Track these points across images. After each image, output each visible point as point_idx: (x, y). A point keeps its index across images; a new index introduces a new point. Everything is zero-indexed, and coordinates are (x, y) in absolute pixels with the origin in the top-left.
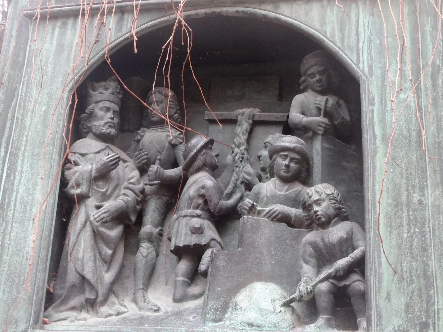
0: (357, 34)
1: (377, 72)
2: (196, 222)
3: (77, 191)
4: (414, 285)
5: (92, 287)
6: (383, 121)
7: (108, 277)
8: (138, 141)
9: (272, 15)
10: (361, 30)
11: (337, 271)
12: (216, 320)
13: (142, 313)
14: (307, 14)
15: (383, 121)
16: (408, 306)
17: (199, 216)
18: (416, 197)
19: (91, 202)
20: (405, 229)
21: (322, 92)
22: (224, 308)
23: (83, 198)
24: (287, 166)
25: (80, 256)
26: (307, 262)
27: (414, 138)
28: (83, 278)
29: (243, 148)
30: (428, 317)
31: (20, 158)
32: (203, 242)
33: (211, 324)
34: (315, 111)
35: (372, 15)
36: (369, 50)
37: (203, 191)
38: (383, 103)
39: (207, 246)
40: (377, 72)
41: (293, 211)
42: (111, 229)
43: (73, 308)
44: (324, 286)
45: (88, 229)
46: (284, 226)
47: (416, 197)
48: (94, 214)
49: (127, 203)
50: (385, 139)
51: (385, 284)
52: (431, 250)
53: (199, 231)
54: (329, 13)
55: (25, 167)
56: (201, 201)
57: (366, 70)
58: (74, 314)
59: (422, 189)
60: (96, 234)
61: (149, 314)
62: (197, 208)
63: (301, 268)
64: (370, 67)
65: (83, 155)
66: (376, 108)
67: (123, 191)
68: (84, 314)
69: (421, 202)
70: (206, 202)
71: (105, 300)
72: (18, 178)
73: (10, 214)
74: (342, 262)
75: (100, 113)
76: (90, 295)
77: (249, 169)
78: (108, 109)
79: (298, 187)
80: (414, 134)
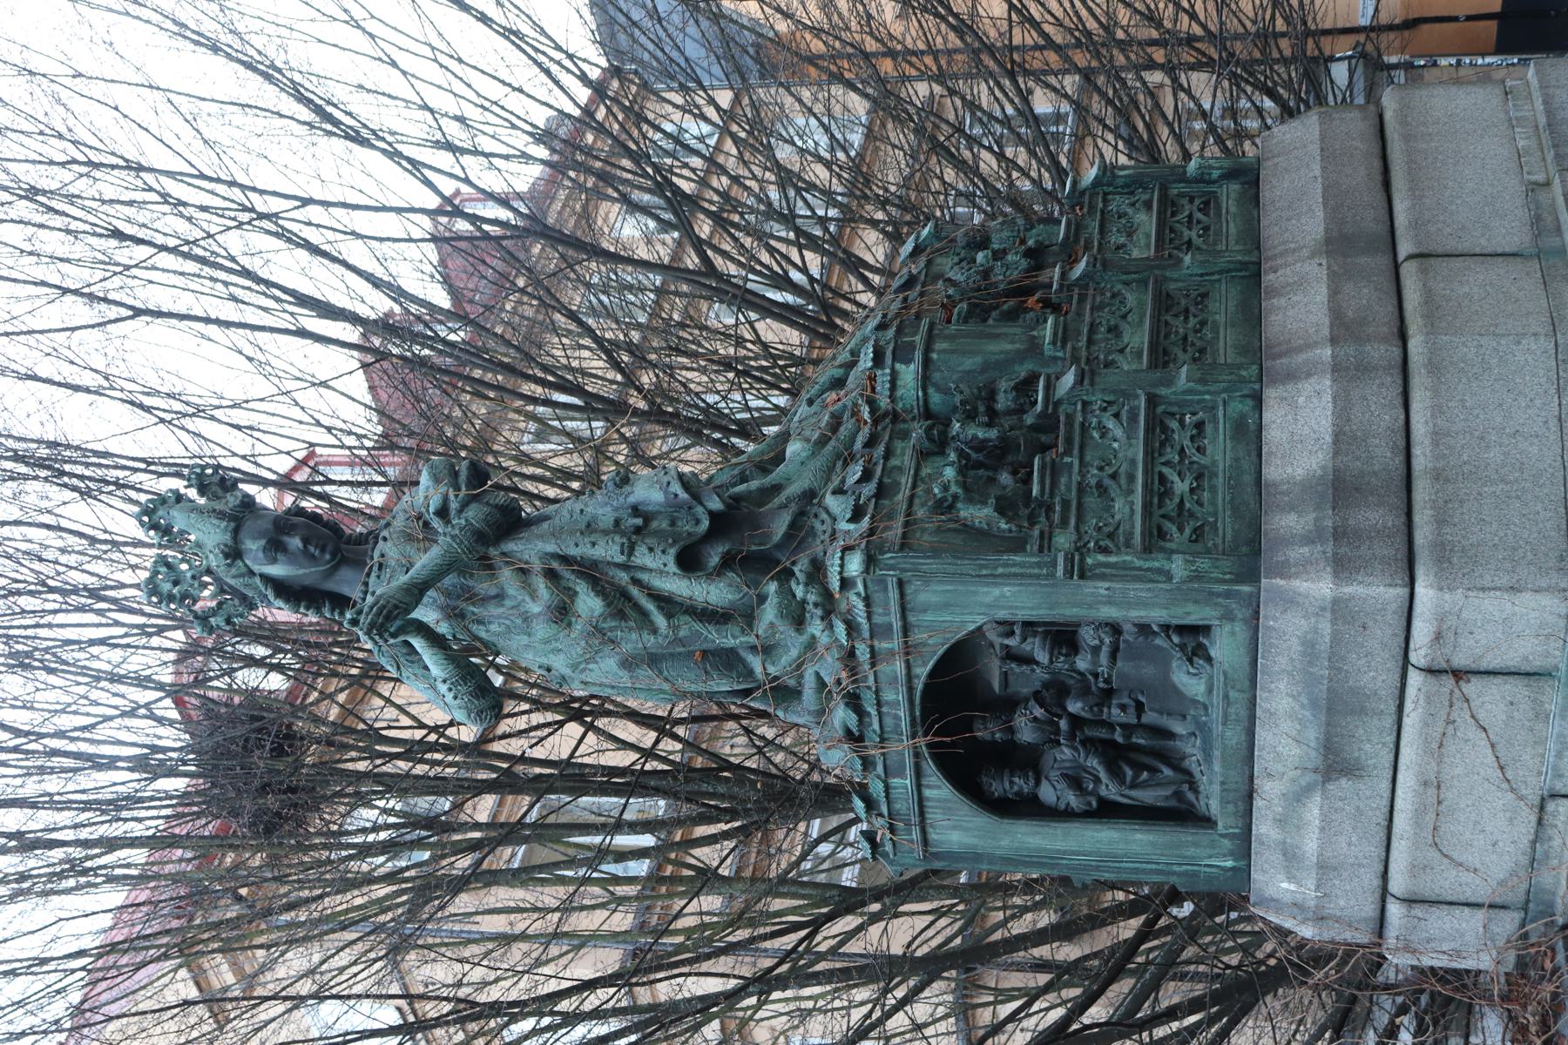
1: (983, 610)
3: (1094, 804)
7: (1167, 772)
16: (1196, 602)
19: (1103, 792)
41: (1105, 650)
42: (1124, 775)
46: (1119, 655)
60: (1133, 786)
68: (1202, 788)
71: (1188, 773)
78: (1012, 783)
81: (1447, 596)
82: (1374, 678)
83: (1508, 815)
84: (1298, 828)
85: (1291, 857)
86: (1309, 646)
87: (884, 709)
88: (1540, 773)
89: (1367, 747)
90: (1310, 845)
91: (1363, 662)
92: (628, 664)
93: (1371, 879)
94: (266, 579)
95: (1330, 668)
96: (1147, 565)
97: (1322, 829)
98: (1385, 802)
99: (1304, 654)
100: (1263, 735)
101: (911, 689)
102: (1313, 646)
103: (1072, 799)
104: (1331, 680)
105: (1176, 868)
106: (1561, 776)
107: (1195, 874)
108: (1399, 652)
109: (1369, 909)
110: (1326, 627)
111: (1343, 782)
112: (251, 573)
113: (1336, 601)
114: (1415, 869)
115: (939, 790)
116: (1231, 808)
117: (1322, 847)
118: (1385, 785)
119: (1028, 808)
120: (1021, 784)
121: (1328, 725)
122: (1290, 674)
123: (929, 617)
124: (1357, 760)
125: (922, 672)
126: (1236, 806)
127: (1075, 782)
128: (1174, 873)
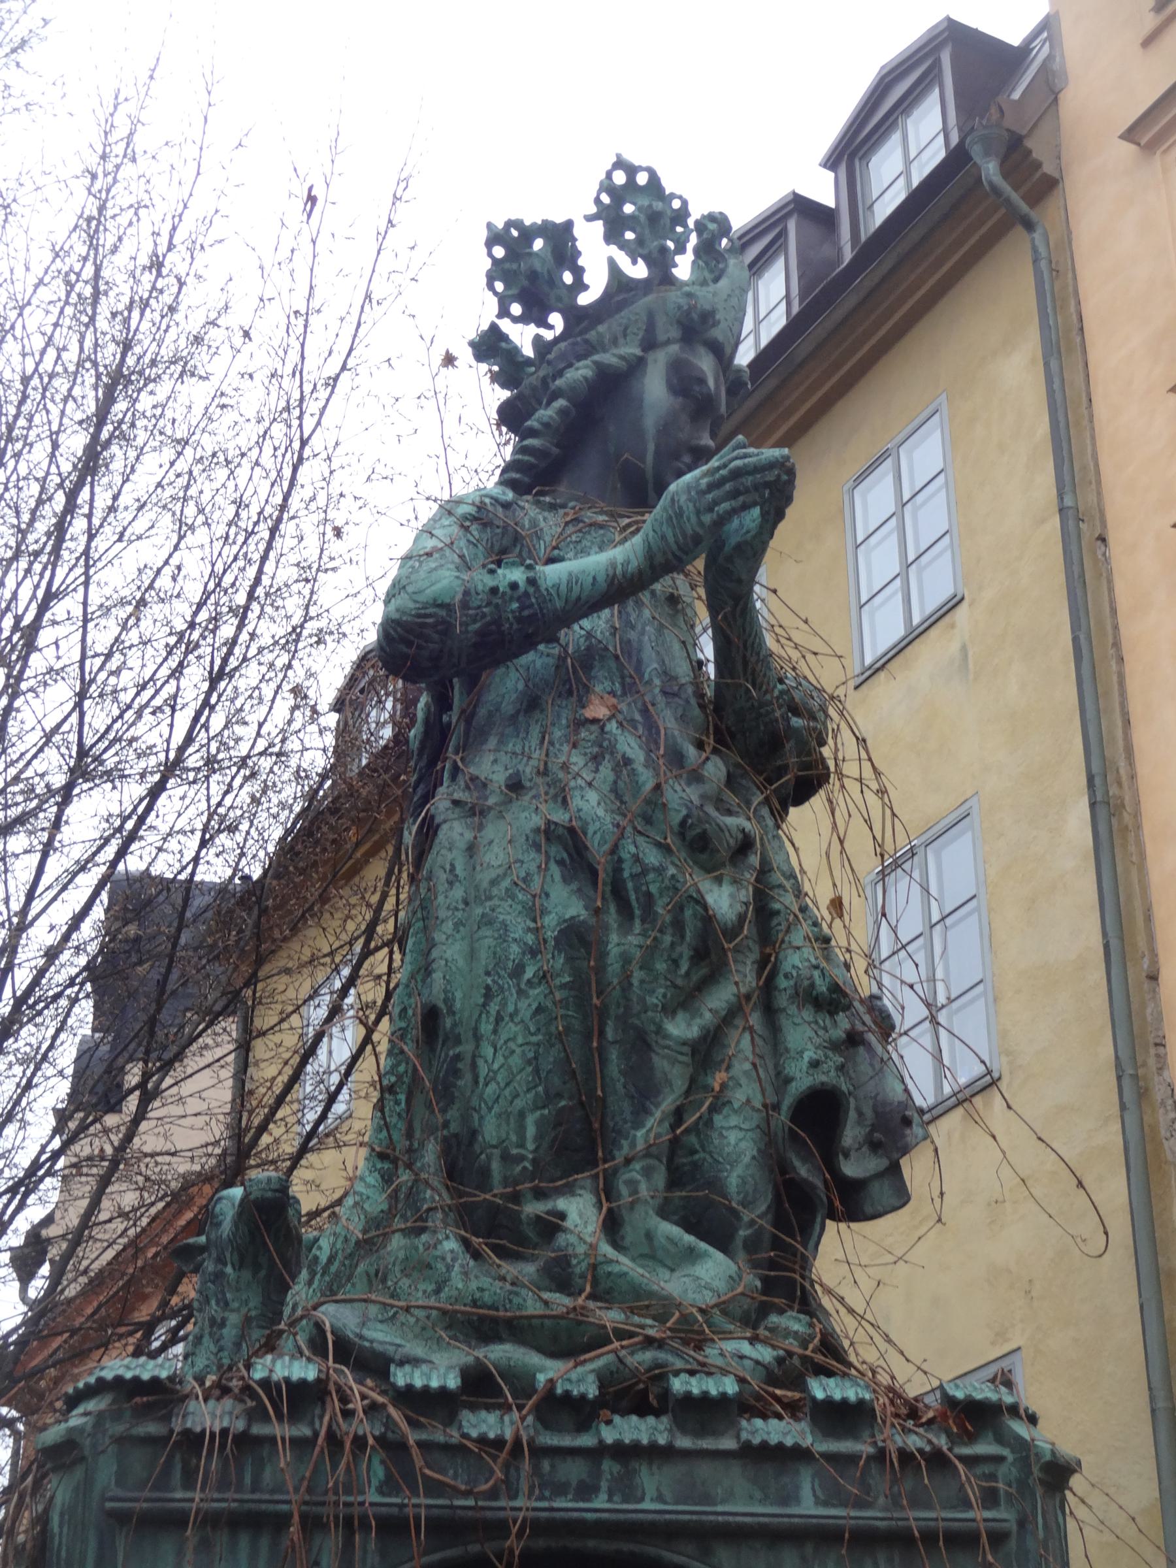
87: (609, 1467)
94: (637, 366)
112: (650, 344)
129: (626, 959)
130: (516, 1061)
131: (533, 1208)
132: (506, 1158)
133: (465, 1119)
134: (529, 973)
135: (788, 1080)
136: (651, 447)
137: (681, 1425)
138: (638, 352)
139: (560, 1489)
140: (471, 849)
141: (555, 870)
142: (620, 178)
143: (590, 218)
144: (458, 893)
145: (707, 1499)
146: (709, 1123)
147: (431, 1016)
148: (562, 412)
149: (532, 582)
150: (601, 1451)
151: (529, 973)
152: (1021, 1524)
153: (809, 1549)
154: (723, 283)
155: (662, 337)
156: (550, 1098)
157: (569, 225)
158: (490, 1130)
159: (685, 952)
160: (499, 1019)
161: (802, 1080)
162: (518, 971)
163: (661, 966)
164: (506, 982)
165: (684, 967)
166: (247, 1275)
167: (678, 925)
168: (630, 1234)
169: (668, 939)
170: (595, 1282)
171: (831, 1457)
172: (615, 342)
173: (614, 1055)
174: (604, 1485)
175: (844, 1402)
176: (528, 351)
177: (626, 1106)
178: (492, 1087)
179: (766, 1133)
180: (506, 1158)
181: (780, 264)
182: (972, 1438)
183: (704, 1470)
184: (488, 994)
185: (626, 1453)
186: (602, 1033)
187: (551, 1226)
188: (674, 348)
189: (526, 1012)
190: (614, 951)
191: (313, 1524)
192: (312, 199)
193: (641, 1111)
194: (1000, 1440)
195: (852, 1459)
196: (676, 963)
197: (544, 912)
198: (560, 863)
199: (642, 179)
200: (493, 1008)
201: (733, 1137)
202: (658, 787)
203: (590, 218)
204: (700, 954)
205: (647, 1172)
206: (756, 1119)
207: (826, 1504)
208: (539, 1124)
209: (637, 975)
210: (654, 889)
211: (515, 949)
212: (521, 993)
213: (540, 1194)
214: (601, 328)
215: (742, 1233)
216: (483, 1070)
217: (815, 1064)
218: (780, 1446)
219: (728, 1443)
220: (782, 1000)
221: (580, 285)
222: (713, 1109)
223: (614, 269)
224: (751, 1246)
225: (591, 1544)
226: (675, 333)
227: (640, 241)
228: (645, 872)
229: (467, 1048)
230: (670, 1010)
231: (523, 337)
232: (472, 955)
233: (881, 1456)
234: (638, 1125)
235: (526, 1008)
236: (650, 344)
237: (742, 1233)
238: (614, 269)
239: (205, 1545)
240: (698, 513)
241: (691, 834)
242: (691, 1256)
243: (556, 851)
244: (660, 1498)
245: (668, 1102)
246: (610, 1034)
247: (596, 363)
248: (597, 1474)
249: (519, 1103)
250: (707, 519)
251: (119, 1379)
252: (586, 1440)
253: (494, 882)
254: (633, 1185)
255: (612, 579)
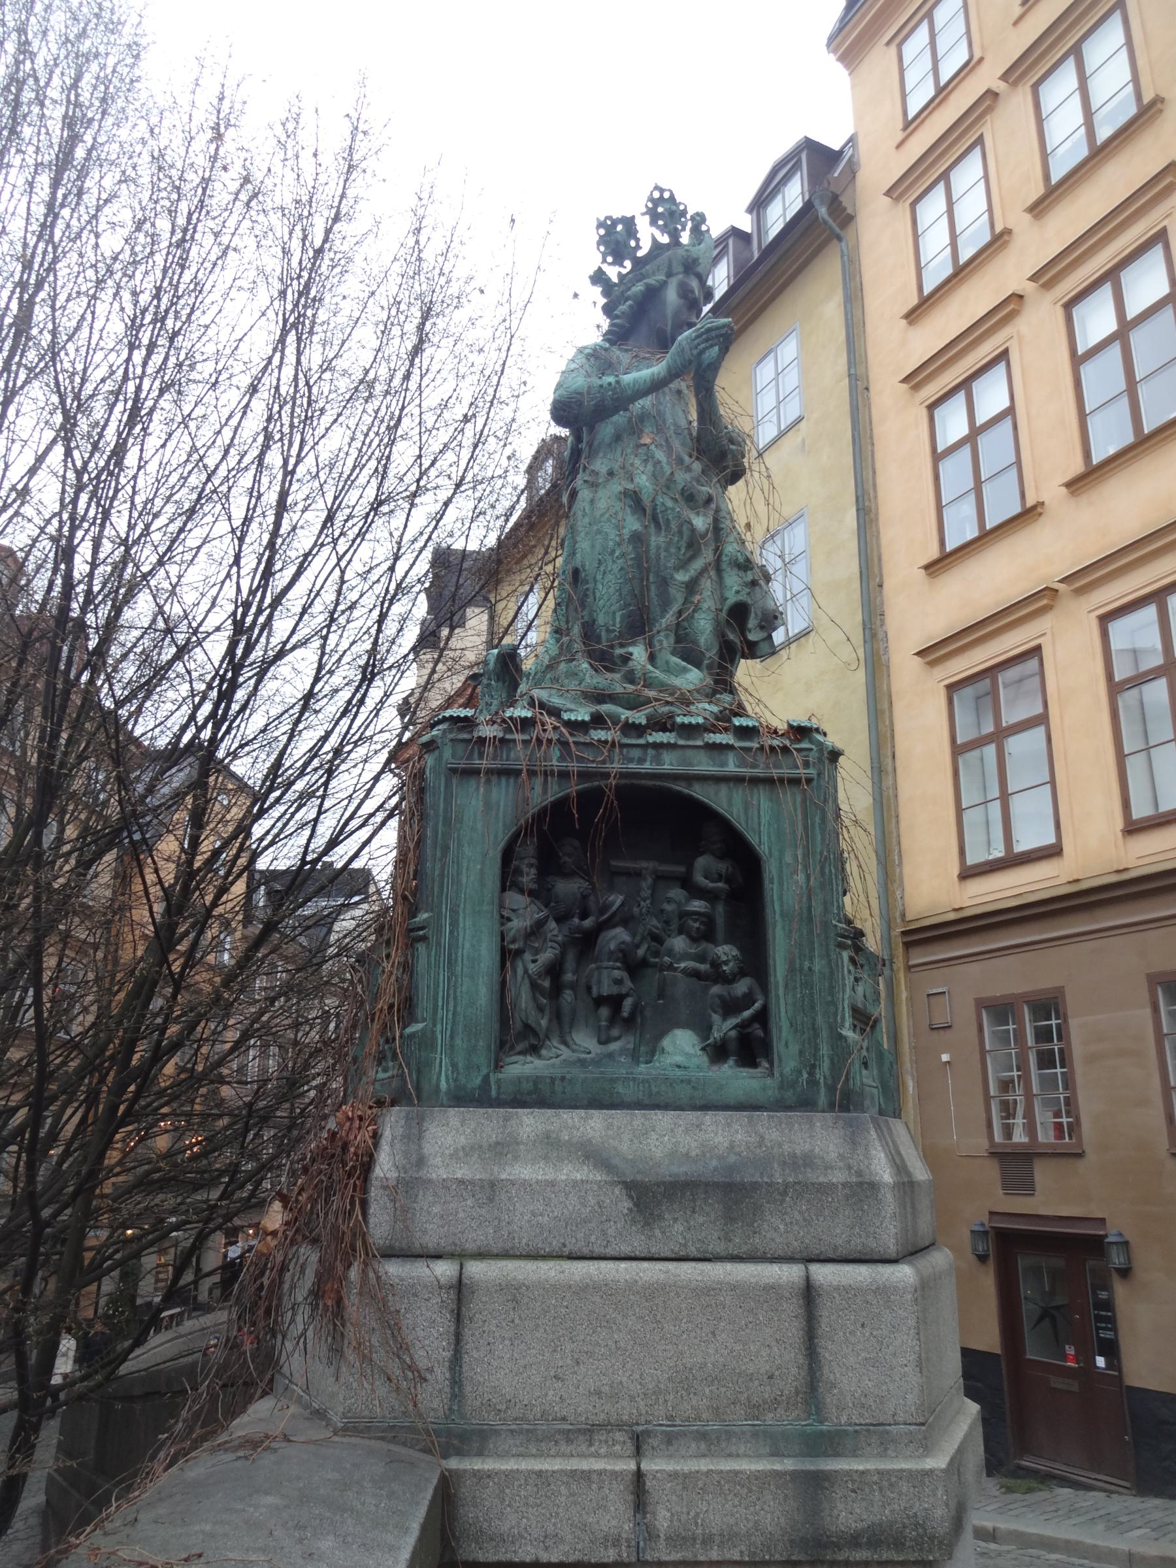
0: (759, 818)
1: (776, 854)
2: (617, 974)
4: (806, 1035)
5: (535, 1034)
6: (781, 898)
8: (549, 890)
9: (686, 791)
10: (762, 813)
11: (743, 1021)
12: (647, 1062)
13: (575, 1055)
14: (716, 794)
15: (781, 898)
16: (801, 1052)
17: (618, 968)
18: (807, 964)
19: (528, 956)
20: (799, 990)
21: (721, 857)
22: (652, 1053)
23: (519, 953)
24: (698, 929)
25: (523, 1006)
26: (715, 1012)
27: (805, 915)
28: (527, 1026)
29: (648, 902)
30: (815, 1060)
31: (461, 915)
32: (624, 991)
33: (643, 1066)
34: (716, 876)
35: (771, 800)
36: (769, 834)
37: (623, 946)
38: (781, 884)
39: (627, 995)
40: (776, 854)
41: (703, 967)
43: (520, 1053)
44: (733, 1033)
45: (527, 981)
46: (694, 980)
47: (807, 964)
48: (532, 968)
49: (555, 955)
50: (782, 914)
51: (784, 1034)
52: (818, 1008)
53: (619, 982)
54: (735, 795)
55: (467, 923)
56: (620, 955)
57: (767, 851)
58: (521, 1057)
59: (811, 959)
60: (534, 986)
61: (583, 1056)
62: (616, 961)
63: (710, 1016)
64: (770, 849)
65: (514, 911)
66: (775, 887)
67: (550, 944)
68: (529, 1058)
69: (810, 969)
70: (625, 956)
72: (461, 934)
73: (459, 969)
74: (747, 1014)
75: (525, 869)
76: (534, 1042)
77: (654, 922)
79: (704, 945)
80: (805, 911)
81: (909, 1297)
82: (776, 1229)
83: (606, 1389)
84: (546, 1158)
85: (503, 1149)
86: (808, 1161)
87: (651, 752)
88: (671, 1418)
89: (679, 1227)
90: (525, 1171)
91: (797, 1216)
92: (637, 539)
93: (473, 1239)
94: (664, 284)
95: (787, 1185)
96: (846, 1010)
97: (552, 1184)
98: (598, 1250)
99: (793, 1156)
100: (663, 1119)
101: (676, 777)
102: (806, 1165)
103: (518, 924)
104: (769, 1185)
105: (439, 1027)
106: (669, 1442)
107: (433, 1046)
108: (815, 1251)
109: (432, 1238)
110: (838, 1177)
111: (626, 1204)
112: (670, 275)
113: (873, 1187)
114: (514, 1293)
115: (540, 795)
116: (527, 1086)
117: (525, 1184)
118: (625, 1249)
119: (508, 879)
120: (528, 877)
121: (707, 1184)
122: (761, 1144)
123: (765, 804)
124: (660, 1217)
125: (699, 792)
126: (530, 1093)
127: (536, 930)
128: (434, 1025)
129: (658, 548)
130: (612, 590)
131: (619, 651)
132: (608, 631)
133: (590, 615)
134: (617, 553)
135: (726, 599)
136: (670, 323)
137: (680, 736)
138: (664, 278)
139: (631, 760)
140: (592, 501)
141: (628, 510)
142: (656, 195)
143: (643, 214)
144: (587, 520)
145: (691, 765)
146: (692, 617)
147: (576, 573)
148: (630, 306)
149: (618, 382)
150: (648, 745)
151: (617, 553)
152: (819, 775)
153: (732, 784)
154: (702, 245)
155: (675, 271)
156: (626, 605)
157: (633, 217)
158: (601, 620)
159: (683, 544)
160: (604, 573)
161: (732, 599)
162: (613, 551)
163: (673, 550)
164: (607, 557)
165: (683, 551)
166: (500, 684)
167: (680, 533)
168: (659, 662)
169: (676, 539)
170: (645, 680)
171: (742, 748)
172: (654, 274)
173: (653, 588)
174: (649, 759)
175: (747, 727)
176: (615, 279)
177: (658, 609)
178: (601, 603)
179: (717, 621)
180: (608, 631)
181: (725, 260)
182: (799, 741)
183: (689, 753)
184: (600, 562)
185: (658, 746)
186: (648, 579)
187: (626, 659)
188: (681, 276)
189: (616, 570)
190: (653, 544)
191: (532, 773)
192: (513, 221)
193: (664, 611)
194: (811, 742)
195: (749, 749)
196: (679, 549)
197: (623, 528)
198: (630, 506)
199: (666, 195)
200: (602, 569)
201: (702, 622)
202: (672, 473)
203: (643, 214)
204: (690, 545)
205: (667, 637)
206: (712, 615)
207: (739, 767)
208: (622, 617)
209: (663, 554)
210: (670, 517)
211: (611, 543)
212: (614, 562)
213: (622, 646)
214: (648, 267)
215: (706, 662)
216: (598, 595)
217: (738, 592)
218: (721, 744)
219: (699, 743)
220: (724, 566)
221: (638, 247)
222: (694, 611)
223: (654, 240)
224: (709, 667)
225: (643, 782)
226: (681, 269)
227: (665, 225)
228: (666, 510)
229: (591, 586)
230: (677, 569)
231: (613, 273)
232: (593, 546)
233: (762, 748)
234: (663, 617)
235: (615, 568)
236: (670, 275)
237: (706, 662)
238: (654, 240)
239: (488, 781)
240: (691, 349)
241: (686, 494)
242: (685, 670)
243: (629, 502)
244: (671, 764)
245: (675, 608)
246: (651, 579)
247: (646, 284)
248: (646, 754)
249: (613, 608)
250: (695, 352)
251: (451, 717)
252: (642, 741)
253: (602, 515)
254: (660, 641)
255: (653, 381)
